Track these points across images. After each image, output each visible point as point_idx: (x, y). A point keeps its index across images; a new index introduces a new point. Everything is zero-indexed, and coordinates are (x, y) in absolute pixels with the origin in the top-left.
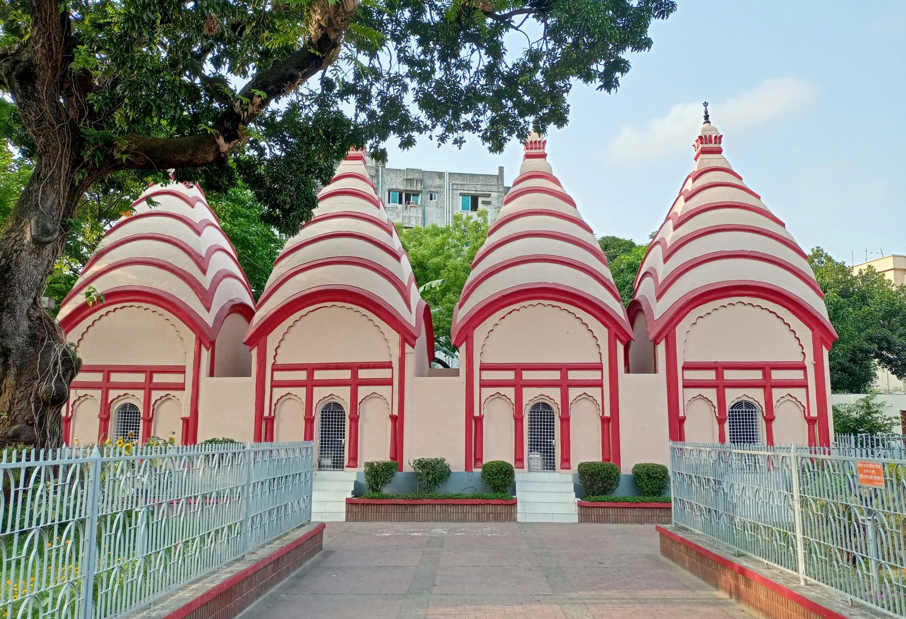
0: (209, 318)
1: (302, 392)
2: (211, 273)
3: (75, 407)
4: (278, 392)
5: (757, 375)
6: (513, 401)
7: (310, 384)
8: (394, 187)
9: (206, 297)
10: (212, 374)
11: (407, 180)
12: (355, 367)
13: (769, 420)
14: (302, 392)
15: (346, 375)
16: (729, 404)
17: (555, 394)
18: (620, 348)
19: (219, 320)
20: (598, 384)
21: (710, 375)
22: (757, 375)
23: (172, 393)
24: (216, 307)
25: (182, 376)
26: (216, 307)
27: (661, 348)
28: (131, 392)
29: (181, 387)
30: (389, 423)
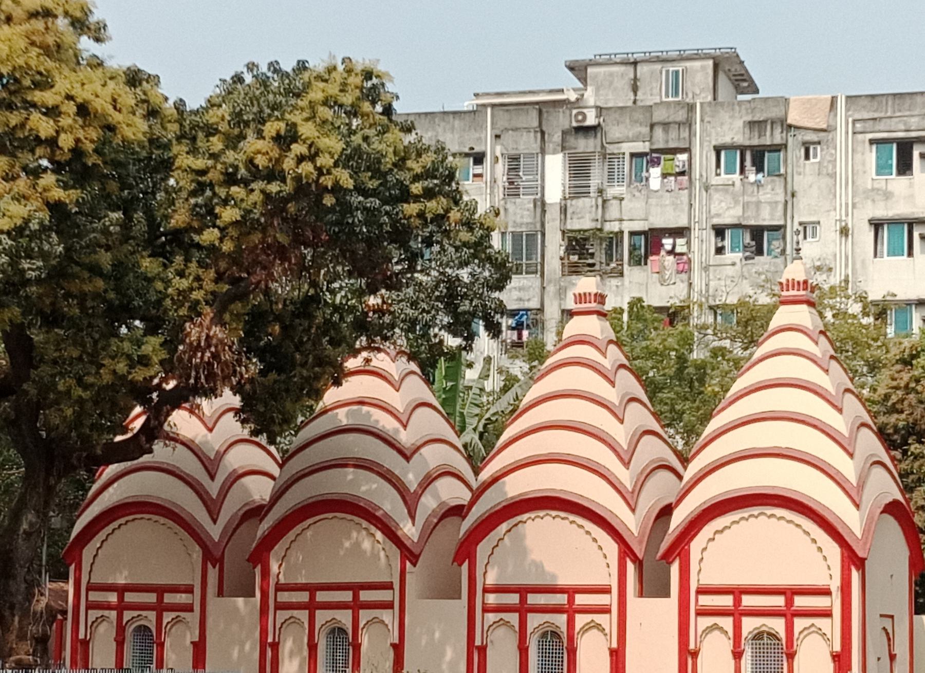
0: (215, 531)
1: (303, 615)
2: (221, 477)
3: (93, 629)
4: (282, 615)
5: (779, 601)
6: (517, 629)
7: (312, 607)
8: (727, 140)
9: (213, 507)
10: (220, 593)
11: (752, 124)
12: (356, 588)
13: (791, 656)
14: (303, 615)
15: (347, 596)
16: (745, 633)
17: (561, 620)
18: (631, 567)
19: (231, 532)
20: (606, 610)
21: (727, 601)
22: (779, 601)
23: (182, 614)
24: (224, 517)
25: (190, 595)
26: (224, 517)
27: (675, 569)
28: (144, 613)
29: (189, 608)
30: (391, 654)
